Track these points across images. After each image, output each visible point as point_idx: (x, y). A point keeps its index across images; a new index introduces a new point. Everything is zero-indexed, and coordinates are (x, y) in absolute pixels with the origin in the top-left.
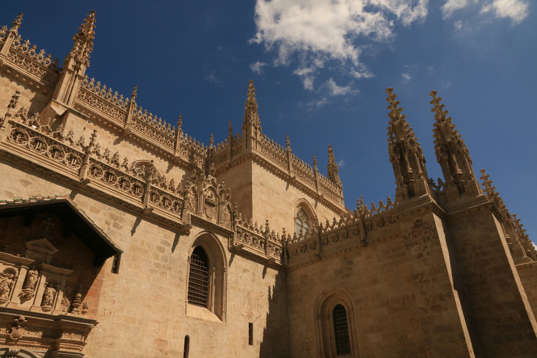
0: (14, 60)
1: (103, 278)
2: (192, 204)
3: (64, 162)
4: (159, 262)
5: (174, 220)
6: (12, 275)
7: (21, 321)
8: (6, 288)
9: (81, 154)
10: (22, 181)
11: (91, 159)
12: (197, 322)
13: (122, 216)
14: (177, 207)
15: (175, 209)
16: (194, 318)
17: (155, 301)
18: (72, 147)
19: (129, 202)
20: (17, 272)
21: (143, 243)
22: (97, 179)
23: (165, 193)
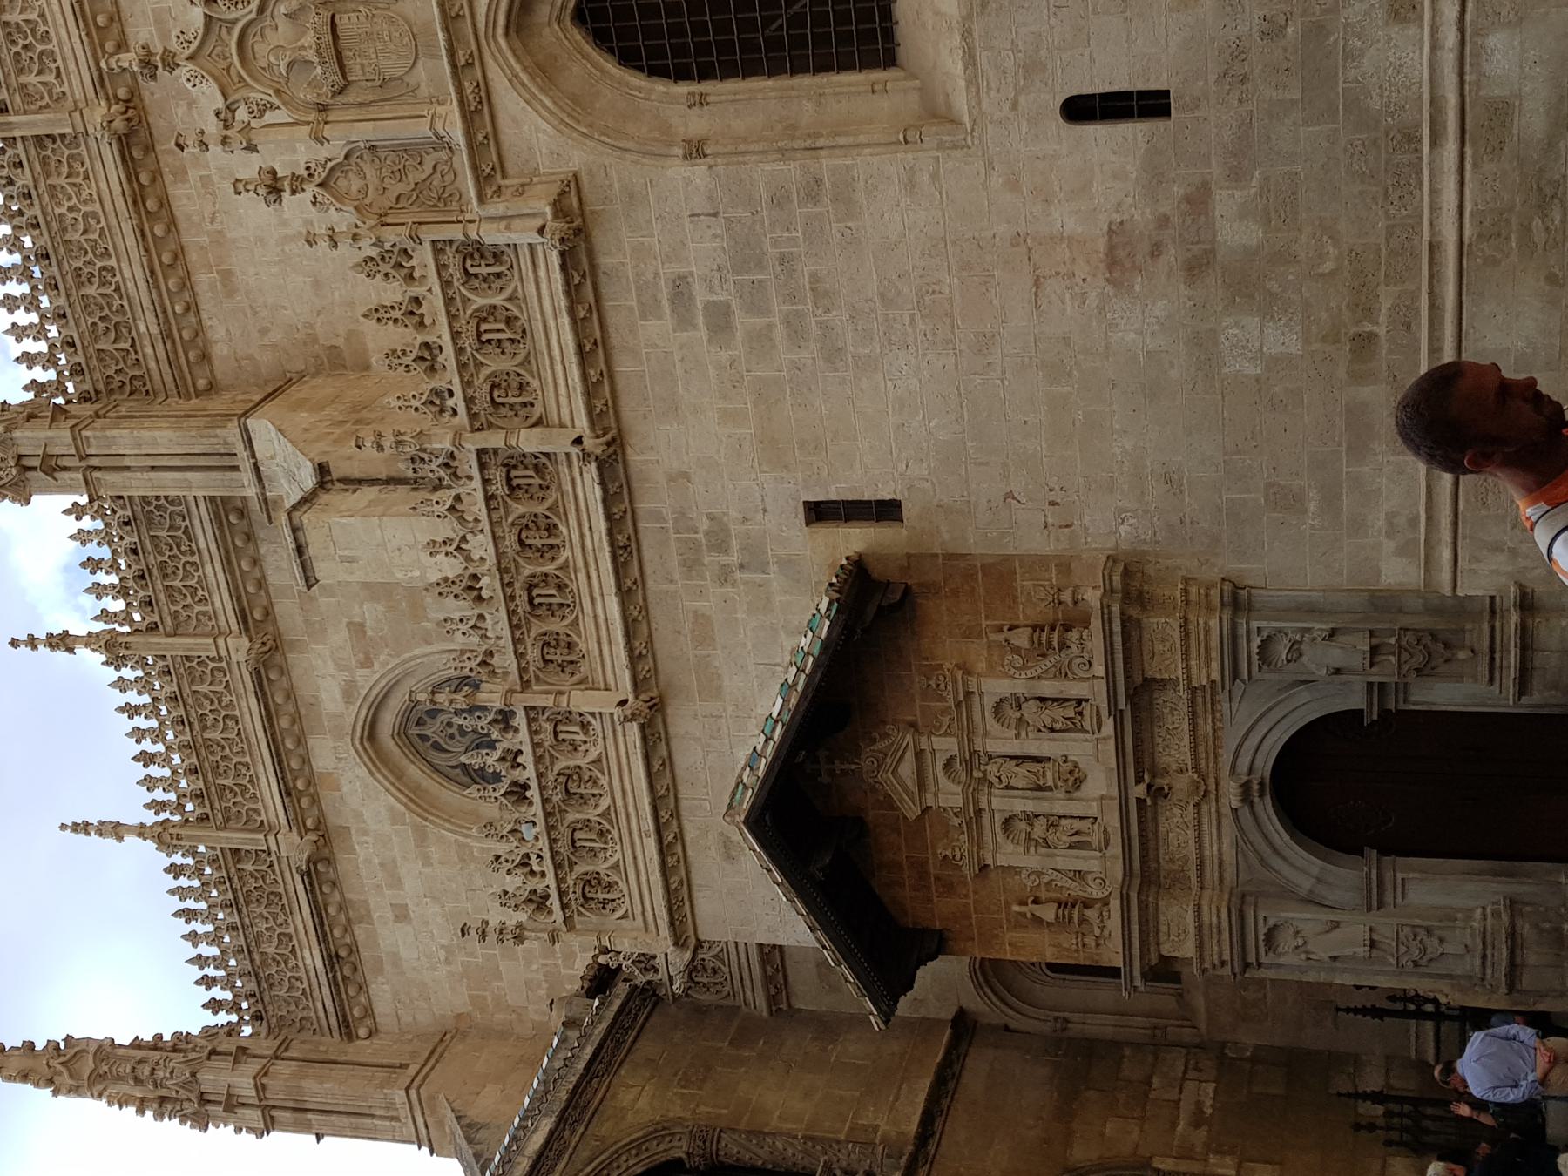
0: (197, 608)
1: (936, 555)
2: (414, 176)
3: (598, 761)
4: (776, 320)
5: (563, 303)
7: (1149, 786)
9: (530, 721)
10: (730, 858)
11: (526, 685)
12: (983, 58)
13: (670, 525)
14: (484, 270)
15: (498, 275)
16: (971, 82)
17: (950, 315)
18: (527, 749)
19: (601, 525)
21: (728, 417)
22: (587, 644)
23: (459, 351)
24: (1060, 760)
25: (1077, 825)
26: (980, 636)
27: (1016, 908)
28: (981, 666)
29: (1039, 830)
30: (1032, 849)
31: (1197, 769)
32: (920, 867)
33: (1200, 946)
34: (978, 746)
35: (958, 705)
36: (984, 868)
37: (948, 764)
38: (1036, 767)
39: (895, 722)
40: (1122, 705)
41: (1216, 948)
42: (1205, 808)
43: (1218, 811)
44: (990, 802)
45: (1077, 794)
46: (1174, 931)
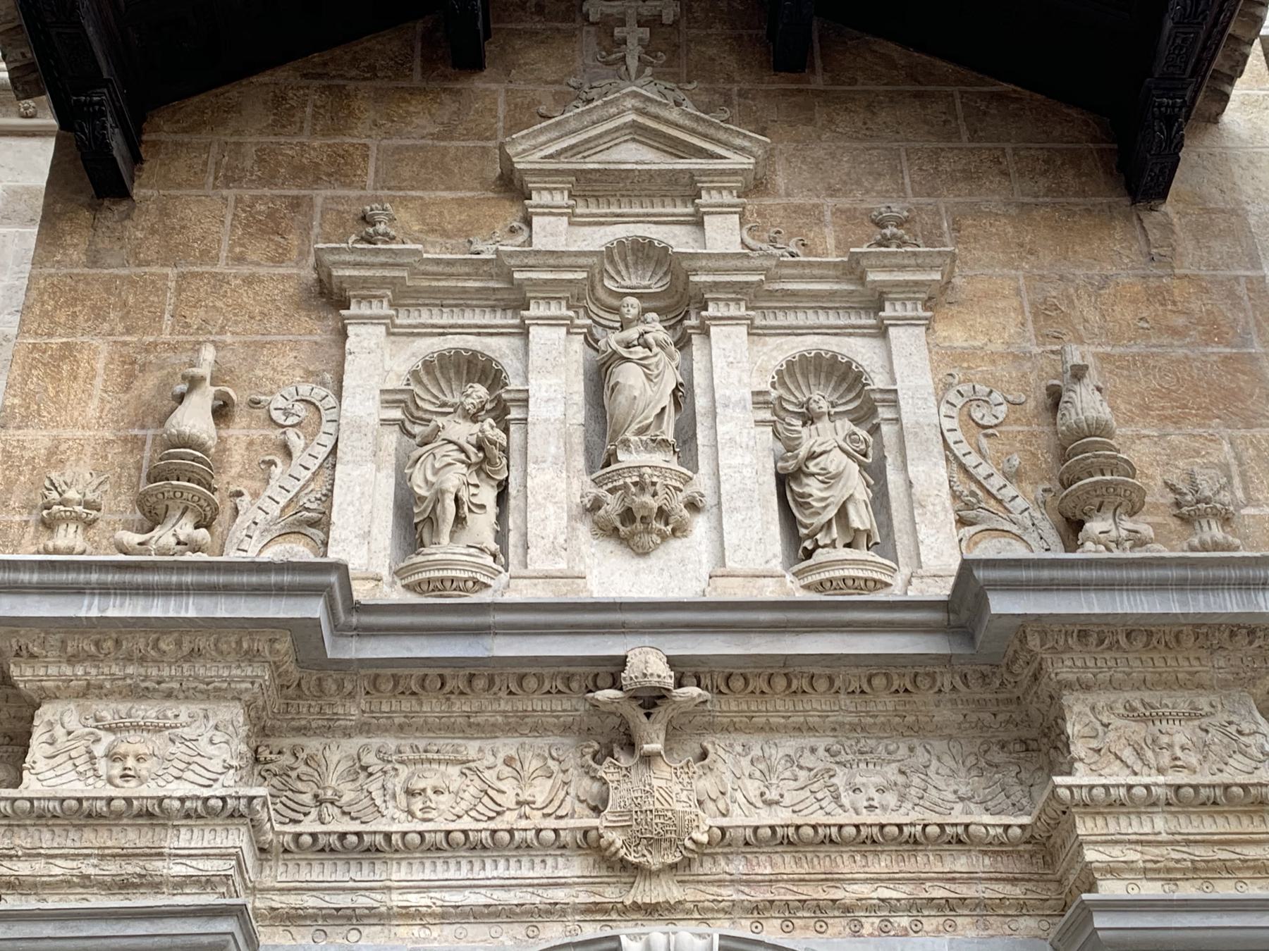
1: (1255, 263)
6: (479, 392)
7: (651, 700)
8: (454, 478)
20: (510, 365)
24: (688, 491)
25: (482, 525)
26: (1043, 337)
27: (208, 354)
28: (955, 335)
29: (462, 431)
30: (397, 414)
31: (723, 841)
32: (341, 168)
33: (82, 815)
34: (712, 310)
35: (853, 269)
36: (330, 297)
37: (644, 253)
38: (670, 437)
39: (770, 154)
40: (1000, 604)
41: (59, 869)
42: (573, 867)
43: (553, 911)
44: (552, 322)
45: (584, 530)
46: (134, 744)
